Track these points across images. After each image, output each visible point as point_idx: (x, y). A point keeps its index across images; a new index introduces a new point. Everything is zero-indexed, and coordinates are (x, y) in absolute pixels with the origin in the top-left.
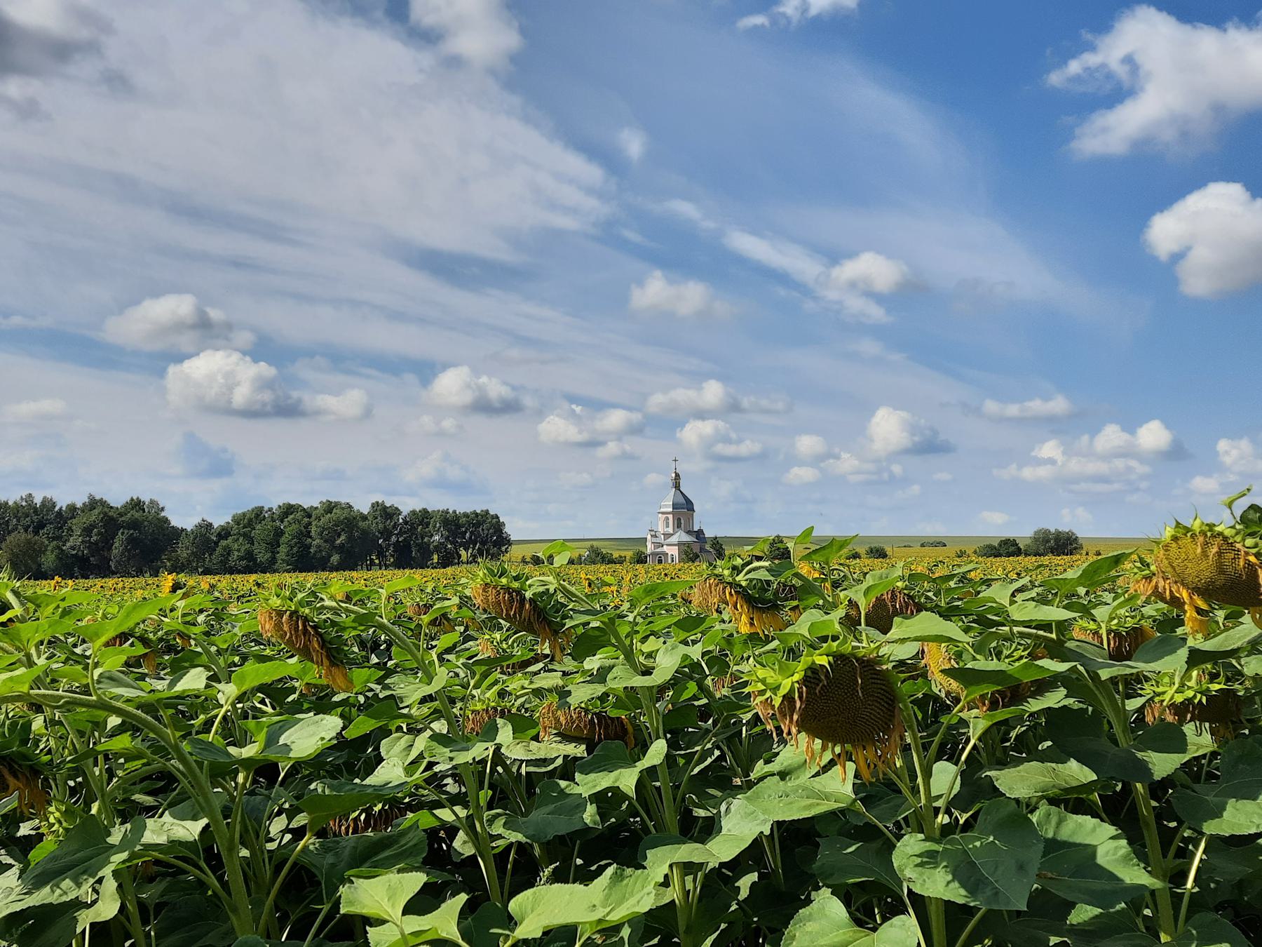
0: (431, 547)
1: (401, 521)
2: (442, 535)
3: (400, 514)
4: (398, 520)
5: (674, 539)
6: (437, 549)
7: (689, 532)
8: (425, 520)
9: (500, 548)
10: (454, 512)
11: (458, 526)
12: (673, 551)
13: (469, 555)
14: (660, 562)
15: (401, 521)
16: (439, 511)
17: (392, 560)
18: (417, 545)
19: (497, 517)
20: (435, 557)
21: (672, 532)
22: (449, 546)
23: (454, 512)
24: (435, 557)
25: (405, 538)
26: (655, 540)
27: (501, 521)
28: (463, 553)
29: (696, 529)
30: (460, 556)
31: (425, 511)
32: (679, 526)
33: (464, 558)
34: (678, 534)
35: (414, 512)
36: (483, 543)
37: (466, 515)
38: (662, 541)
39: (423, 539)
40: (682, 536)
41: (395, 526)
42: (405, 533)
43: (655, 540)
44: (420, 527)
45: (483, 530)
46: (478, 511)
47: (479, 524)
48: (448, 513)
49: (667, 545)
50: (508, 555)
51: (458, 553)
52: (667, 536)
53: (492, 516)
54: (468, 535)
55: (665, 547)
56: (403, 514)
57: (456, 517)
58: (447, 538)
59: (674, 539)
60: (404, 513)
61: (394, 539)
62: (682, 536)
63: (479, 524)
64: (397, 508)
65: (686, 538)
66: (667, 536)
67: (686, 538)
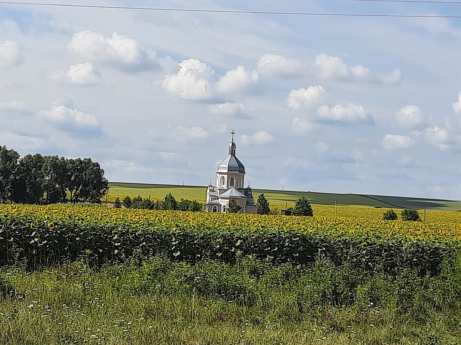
0: (42, 186)
1: (18, 163)
2: (52, 177)
3: (17, 157)
4: (16, 162)
5: (227, 194)
6: (47, 188)
7: (239, 190)
8: (39, 164)
9: (98, 191)
10: (63, 158)
11: (66, 171)
12: (224, 203)
13: (73, 194)
14: (215, 211)
15: (18, 163)
16: (50, 157)
17: (9, 194)
18: (31, 183)
19: (98, 165)
20: (45, 194)
21: (226, 188)
22: (57, 186)
23: (63, 158)
24: (45, 194)
25: (21, 178)
26: (212, 193)
27: (101, 168)
28: (68, 192)
29: (245, 187)
30: (65, 195)
31: (38, 156)
32: (232, 184)
33: (68, 197)
34: (230, 190)
35: (29, 157)
36: (85, 185)
37: (72, 162)
38: (218, 195)
39: (35, 178)
40: (233, 192)
41: (13, 168)
42: (21, 173)
43: (212, 193)
44: (34, 169)
45: (85, 175)
46: (82, 160)
47: (82, 170)
48: (58, 159)
49: (221, 198)
50: (105, 197)
51: (64, 193)
52: (222, 191)
53: (94, 164)
54: (73, 178)
55: (219, 199)
56: (21, 157)
57: (64, 162)
58: (56, 180)
59: (227, 194)
60: (22, 157)
61: (12, 177)
62: (233, 192)
63: (82, 170)
64: (16, 152)
65: (235, 193)
66: (222, 191)
67: (235, 193)
